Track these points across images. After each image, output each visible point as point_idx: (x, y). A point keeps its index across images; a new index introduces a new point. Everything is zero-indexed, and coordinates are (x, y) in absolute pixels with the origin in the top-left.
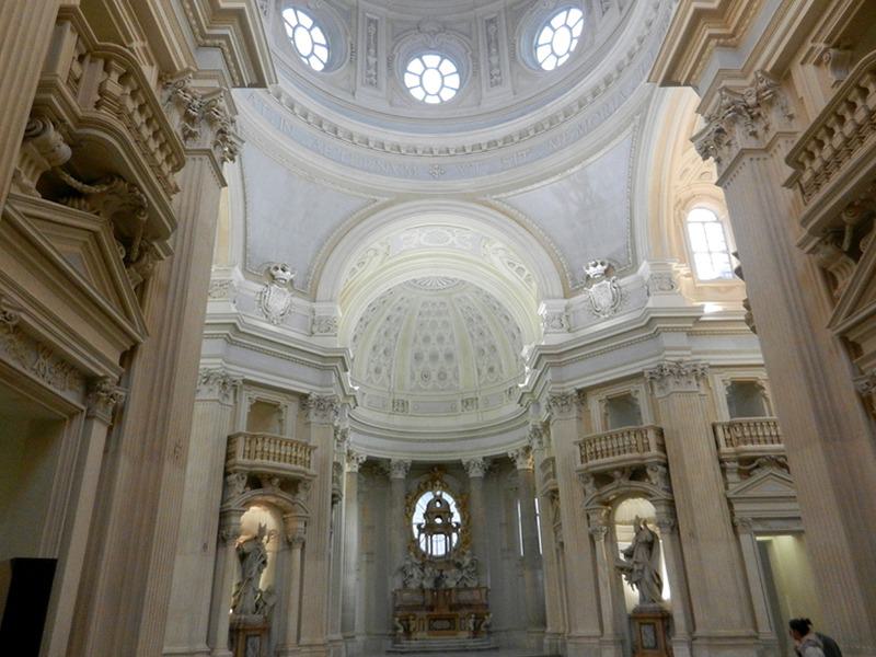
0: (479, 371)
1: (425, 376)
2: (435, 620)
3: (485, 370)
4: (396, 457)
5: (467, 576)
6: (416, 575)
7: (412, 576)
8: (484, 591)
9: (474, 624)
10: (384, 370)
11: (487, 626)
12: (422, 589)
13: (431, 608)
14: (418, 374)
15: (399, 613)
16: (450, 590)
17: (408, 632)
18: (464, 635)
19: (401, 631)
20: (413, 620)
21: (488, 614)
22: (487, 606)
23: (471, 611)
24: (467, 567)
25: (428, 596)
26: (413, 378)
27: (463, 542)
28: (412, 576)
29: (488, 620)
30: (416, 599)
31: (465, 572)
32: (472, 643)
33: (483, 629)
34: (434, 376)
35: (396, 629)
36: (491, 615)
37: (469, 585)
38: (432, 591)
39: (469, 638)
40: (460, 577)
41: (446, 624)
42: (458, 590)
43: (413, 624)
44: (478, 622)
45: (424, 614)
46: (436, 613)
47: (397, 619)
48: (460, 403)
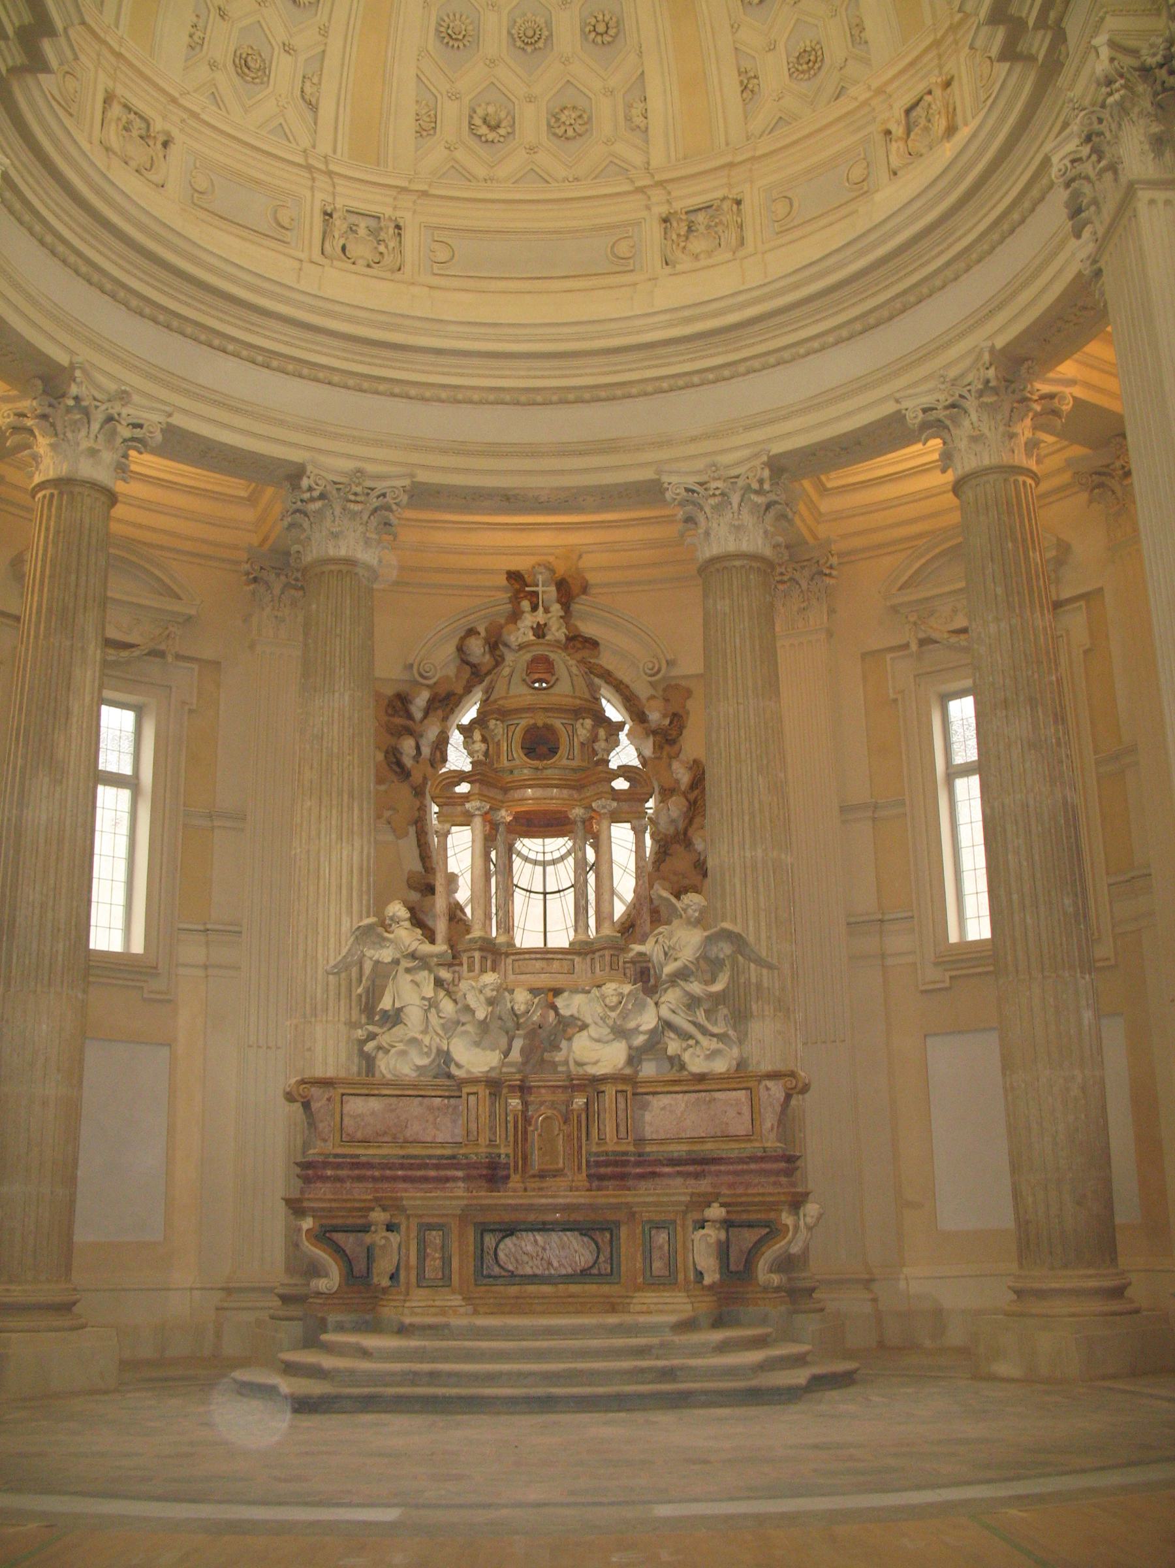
0: (748, 86)
1: (490, 128)
2: (509, 1231)
3: (774, 73)
4: (332, 462)
5: (680, 1021)
6: (414, 1015)
7: (394, 1018)
8: (776, 1090)
9: (723, 1251)
10: (284, 71)
11: (786, 1264)
12: (445, 1081)
13: (493, 1174)
14: (451, 114)
15: (323, 1190)
16: (593, 1084)
17: (361, 1285)
18: (664, 1308)
19: (331, 1281)
20: (390, 1228)
21: (797, 1203)
22: (790, 1162)
23: (704, 1185)
24: (682, 975)
25: (478, 1103)
26: (426, 127)
27: (677, 863)
28: (394, 1018)
29: (799, 1231)
30: (414, 1129)
31: (672, 997)
32: (711, 1355)
33: (764, 1274)
34: (531, 123)
35: (314, 1270)
36: (811, 1209)
37: (696, 1064)
38: (494, 1085)
39: (687, 1325)
40: (648, 1020)
41: (572, 1251)
42: (628, 1083)
43: (391, 1249)
44: (750, 1237)
45: (458, 1195)
46: (513, 1195)
47: (307, 1223)
48: (653, 232)
